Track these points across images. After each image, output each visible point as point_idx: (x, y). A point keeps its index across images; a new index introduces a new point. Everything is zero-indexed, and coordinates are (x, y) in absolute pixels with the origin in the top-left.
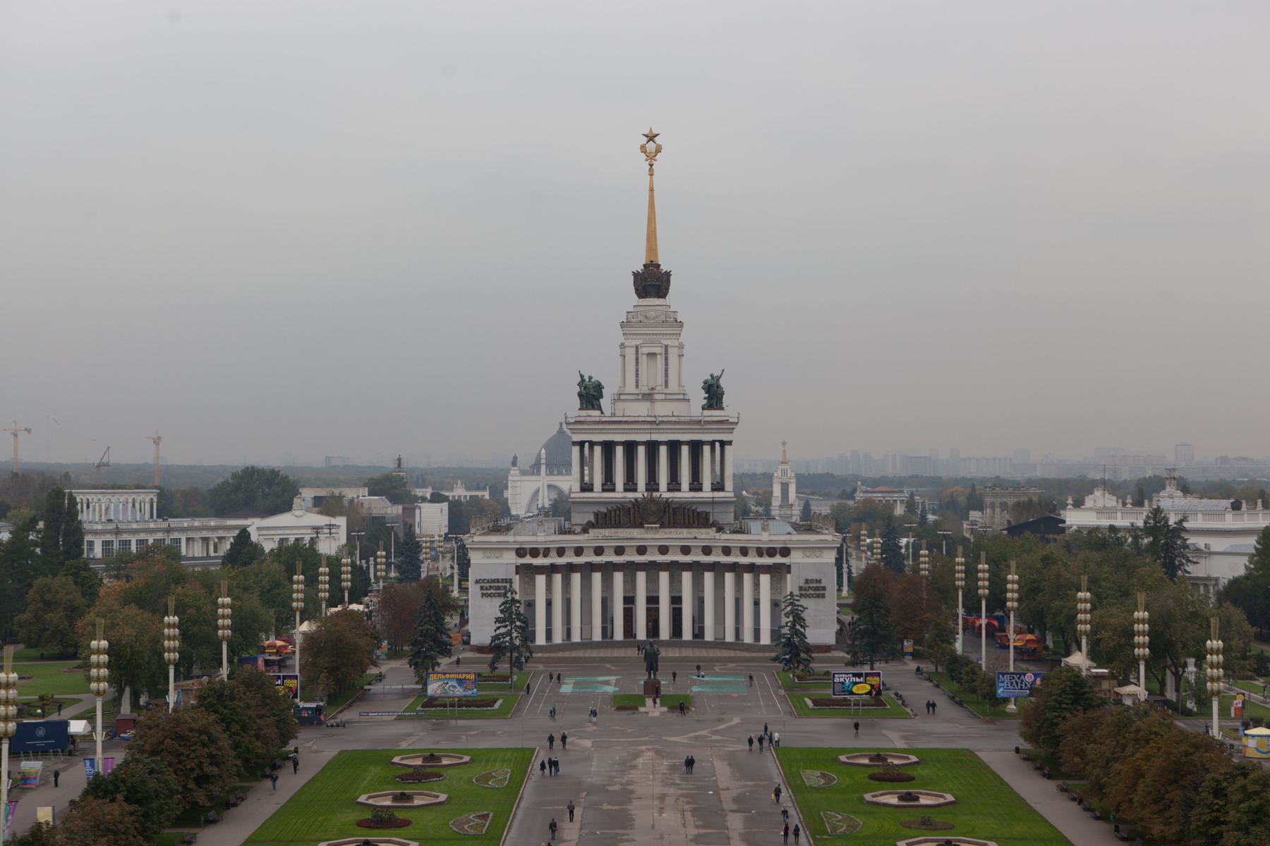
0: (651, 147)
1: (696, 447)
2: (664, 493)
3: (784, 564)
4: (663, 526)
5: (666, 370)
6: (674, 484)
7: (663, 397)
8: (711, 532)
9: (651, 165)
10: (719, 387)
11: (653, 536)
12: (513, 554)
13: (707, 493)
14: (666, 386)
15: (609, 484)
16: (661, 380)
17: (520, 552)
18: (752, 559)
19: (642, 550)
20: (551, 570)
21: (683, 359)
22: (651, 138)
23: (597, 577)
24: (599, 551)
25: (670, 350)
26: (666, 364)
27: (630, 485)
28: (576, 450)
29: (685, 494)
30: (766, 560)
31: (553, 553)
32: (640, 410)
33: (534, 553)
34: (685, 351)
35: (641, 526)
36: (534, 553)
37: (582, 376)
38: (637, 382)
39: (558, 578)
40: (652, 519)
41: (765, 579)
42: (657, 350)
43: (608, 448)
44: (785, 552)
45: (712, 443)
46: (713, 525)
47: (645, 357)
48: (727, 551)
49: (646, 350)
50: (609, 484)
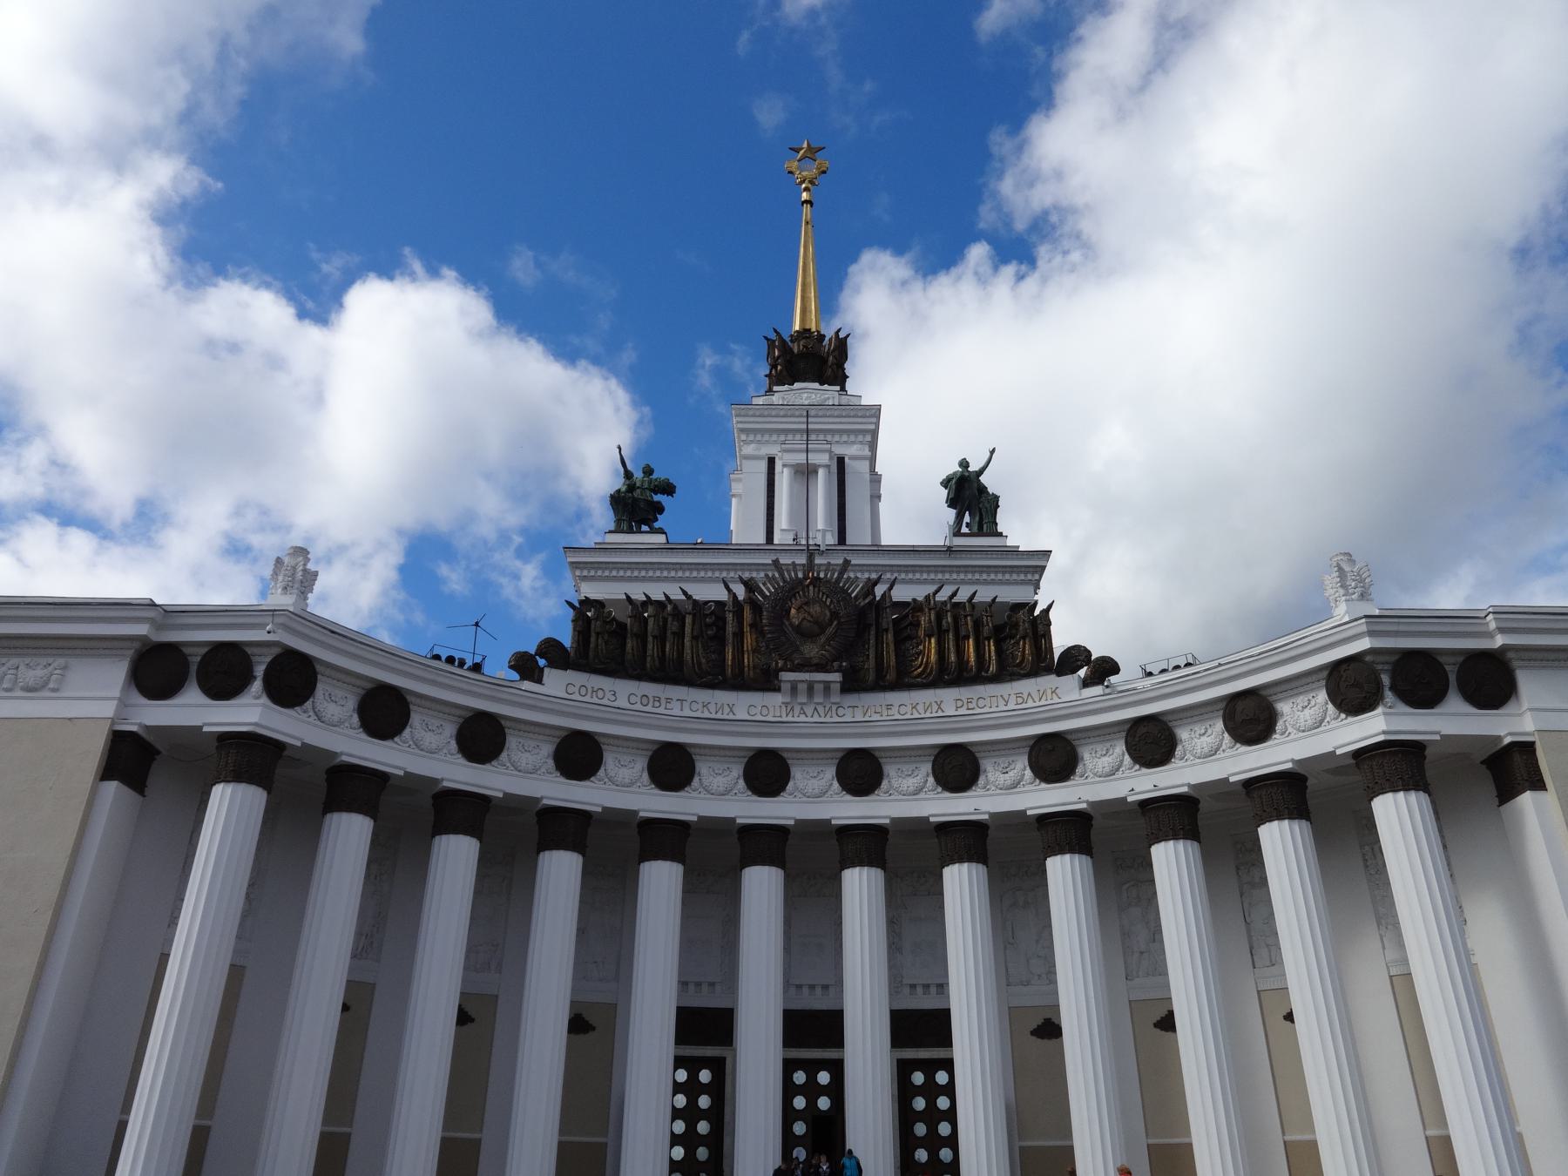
4: (854, 684)
8: (1069, 688)
9: (806, 189)
10: (982, 489)
12: (115, 673)
14: (842, 538)
18: (1313, 733)
19: (767, 772)
23: (560, 873)
24: (579, 755)
35: (766, 682)
36: (224, 669)
37: (628, 475)
39: (349, 837)
40: (811, 650)
44: (1489, 678)
48: (1152, 740)
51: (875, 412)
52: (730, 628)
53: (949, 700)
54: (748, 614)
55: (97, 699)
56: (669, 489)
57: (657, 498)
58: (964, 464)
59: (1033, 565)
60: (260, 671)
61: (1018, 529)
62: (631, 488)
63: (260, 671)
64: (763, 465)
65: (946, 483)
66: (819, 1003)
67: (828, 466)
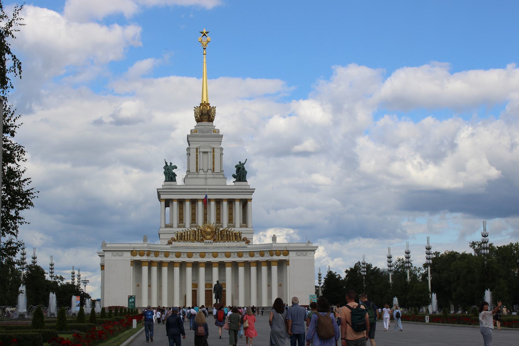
3: (285, 260)
5: (213, 162)
7: (212, 176)
8: (243, 244)
10: (244, 169)
12: (130, 253)
16: (210, 167)
17: (133, 253)
20: (150, 264)
21: (224, 156)
24: (178, 255)
25: (215, 150)
26: (214, 157)
28: (163, 203)
30: (275, 258)
31: (152, 255)
33: (142, 254)
34: (224, 152)
36: (142, 254)
37: (166, 163)
38: (197, 168)
40: (208, 237)
41: (274, 269)
42: (209, 150)
43: (181, 202)
44: (286, 253)
45: (241, 200)
47: (201, 153)
48: (252, 254)
49: (202, 150)
51: (222, 136)
52: (197, 233)
53: (227, 244)
54: (200, 231)
55: (128, 256)
56: (176, 168)
57: (174, 171)
58: (240, 162)
59: (252, 191)
60: (146, 253)
61: (251, 181)
62: (168, 169)
63: (146, 253)
64: (195, 150)
65: (236, 167)
66: (209, 282)
67: (211, 152)
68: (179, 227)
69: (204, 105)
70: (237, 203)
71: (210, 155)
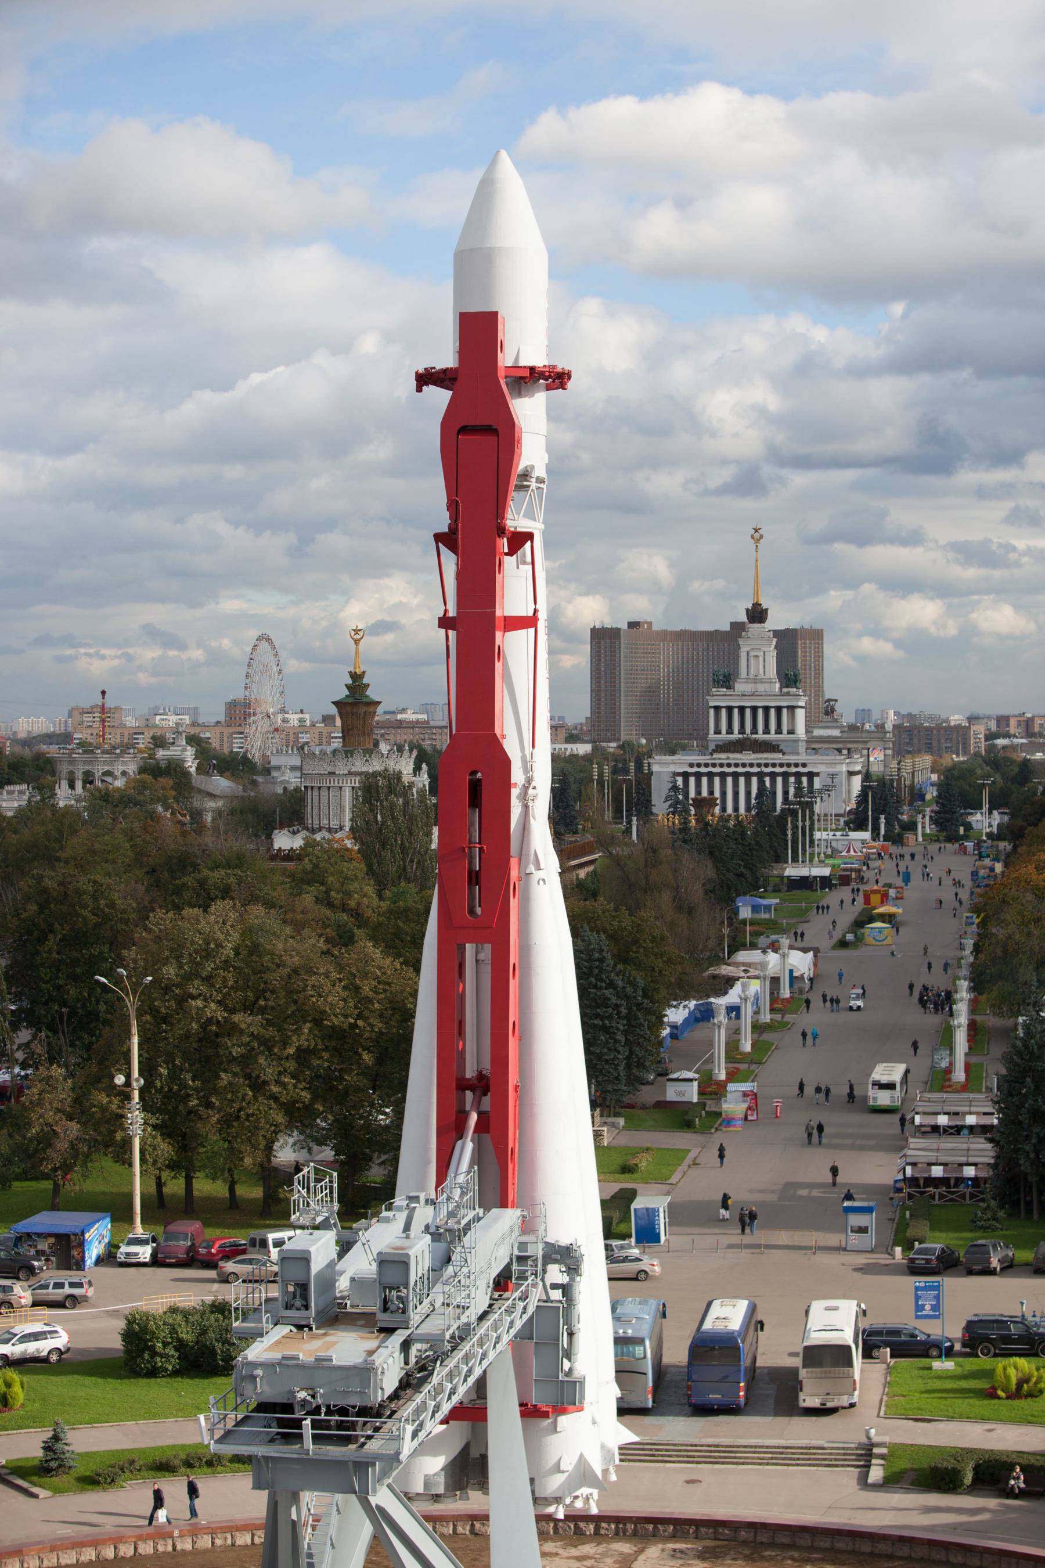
0: (757, 535)
1: (779, 709)
2: (760, 736)
4: (754, 752)
6: (767, 731)
8: (780, 755)
11: (748, 757)
13: (785, 736)
15: (730, 731)
16: (761, 672)
22: (756, 531)
27: (742, 730)
28: (712, 712)
29: (772, 736)
32: (748, 688)
35: (741, 752)
45: (788, 707)
46: (781, 751)
50: (730, 731)
68: (727, 733)
69: (756, 605)
70: (785, 711)
71: (761, 659)
